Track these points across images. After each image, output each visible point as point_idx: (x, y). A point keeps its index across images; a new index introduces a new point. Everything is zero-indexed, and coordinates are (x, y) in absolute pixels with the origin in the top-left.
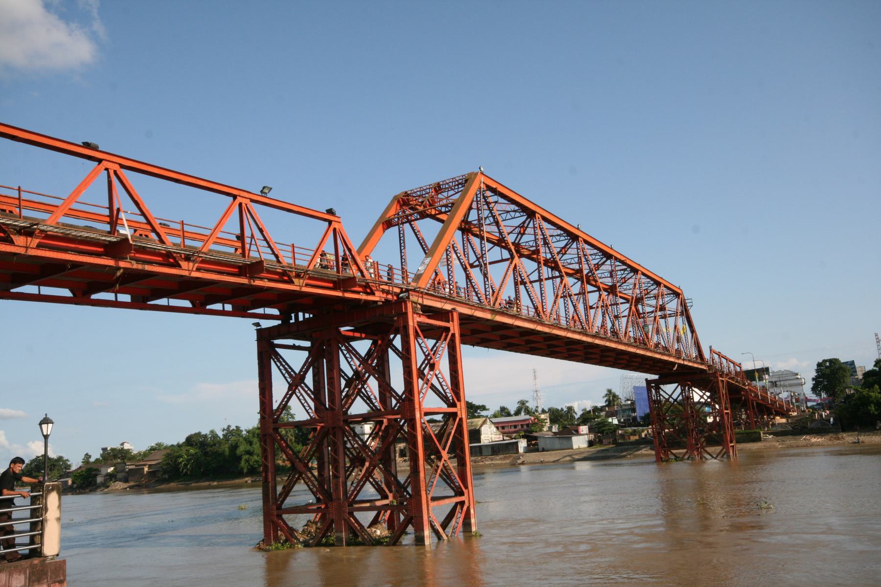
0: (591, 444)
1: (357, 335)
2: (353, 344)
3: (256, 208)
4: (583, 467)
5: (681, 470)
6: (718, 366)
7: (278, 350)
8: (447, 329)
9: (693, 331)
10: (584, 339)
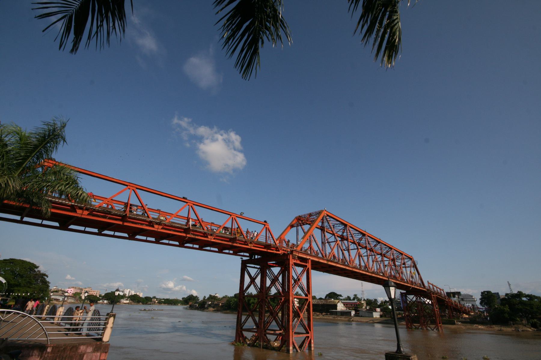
0: (381, 316)
1: (275, 265)
2: (272, 269)
3: (238, 219)
4: (378, 326)
5: (418, 334)
6: (432, 290)
8: (306, 266)
9: (419, 274)
10: (367, 274)
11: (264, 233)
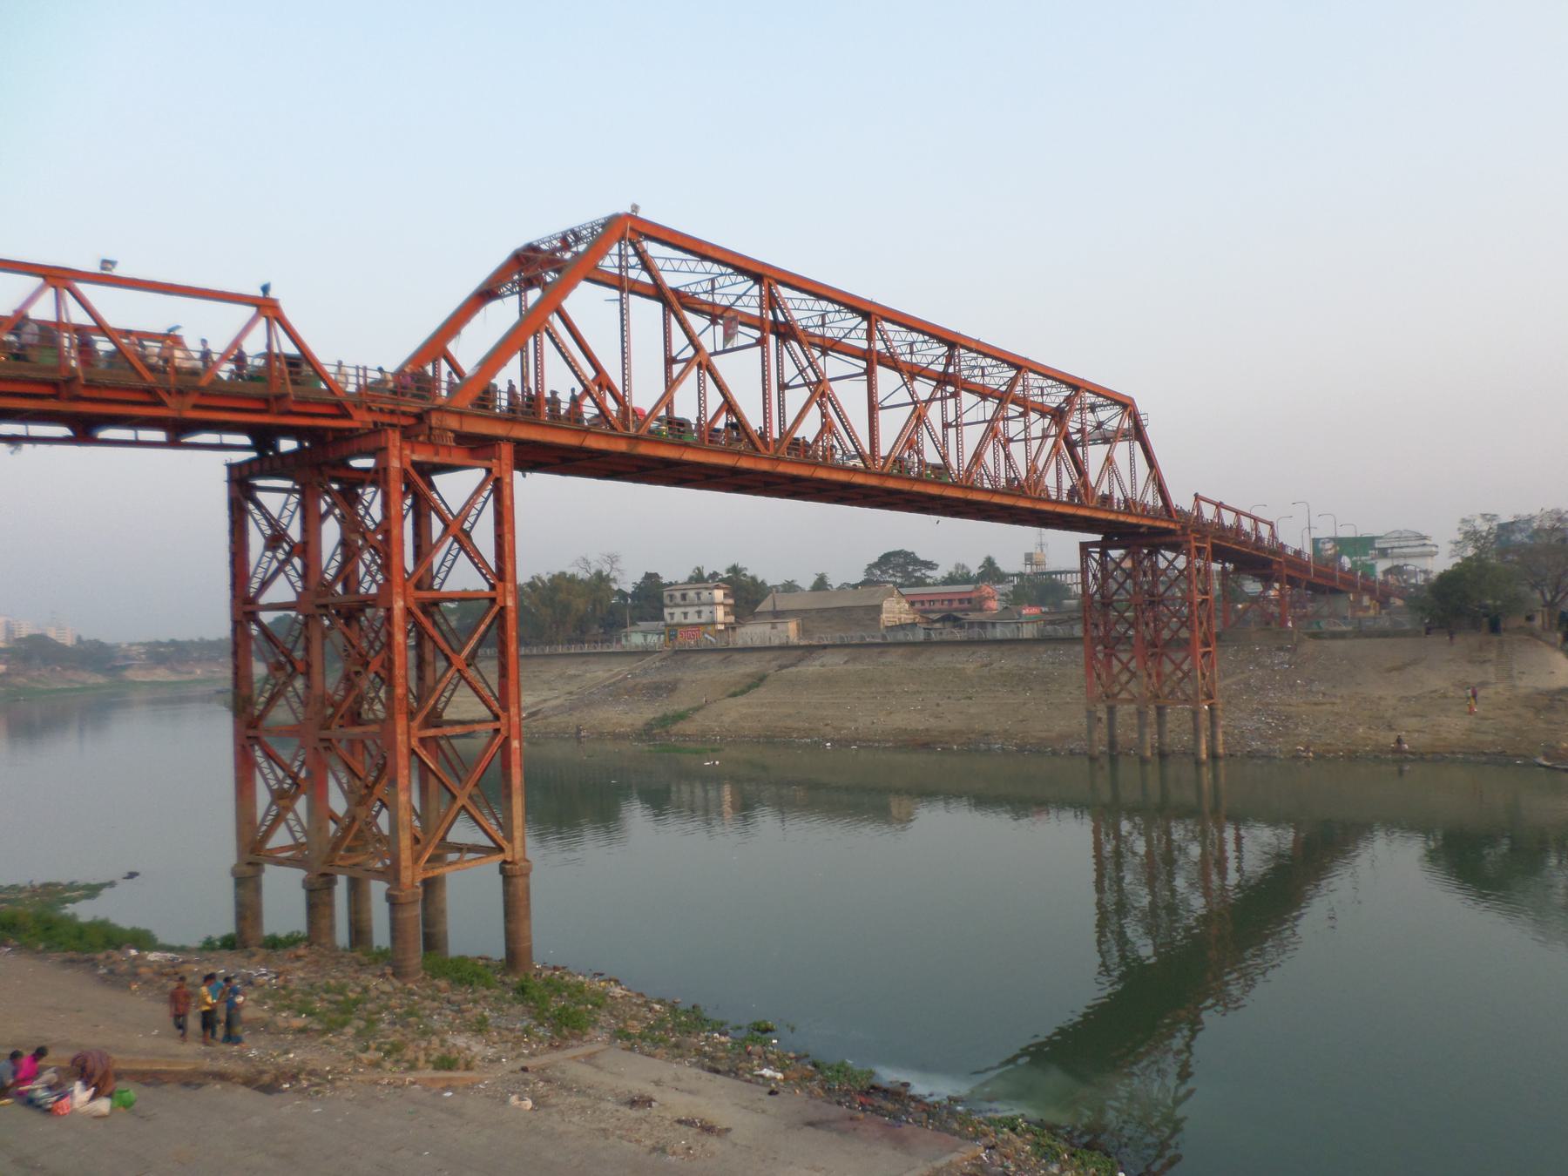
7: (260, 496)
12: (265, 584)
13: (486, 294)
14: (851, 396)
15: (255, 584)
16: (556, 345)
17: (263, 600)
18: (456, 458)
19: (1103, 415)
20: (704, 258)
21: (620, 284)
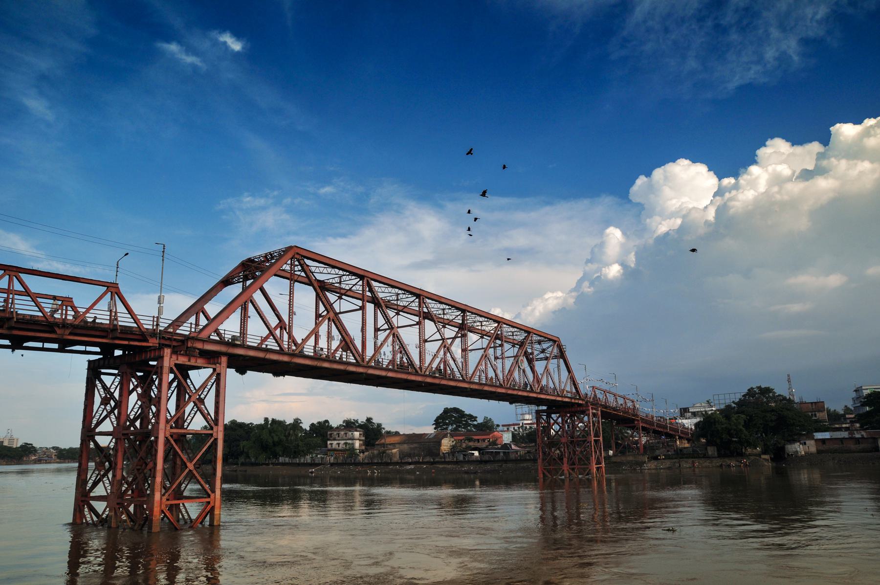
7: (103, 377)
9: (569, 371)
11: (104, 304)
12: (99, 423)
13: (226, 282)
14: (410, 337)
15: (94, 421)
16: (255, 308)
17: (97, 430)
18: (200, 362)
19: (545, 346)
20: (333, 267)
21: (292, 278)
